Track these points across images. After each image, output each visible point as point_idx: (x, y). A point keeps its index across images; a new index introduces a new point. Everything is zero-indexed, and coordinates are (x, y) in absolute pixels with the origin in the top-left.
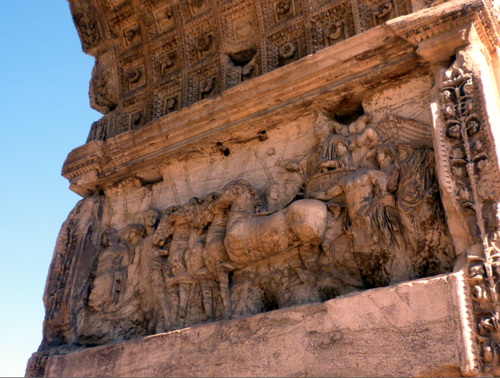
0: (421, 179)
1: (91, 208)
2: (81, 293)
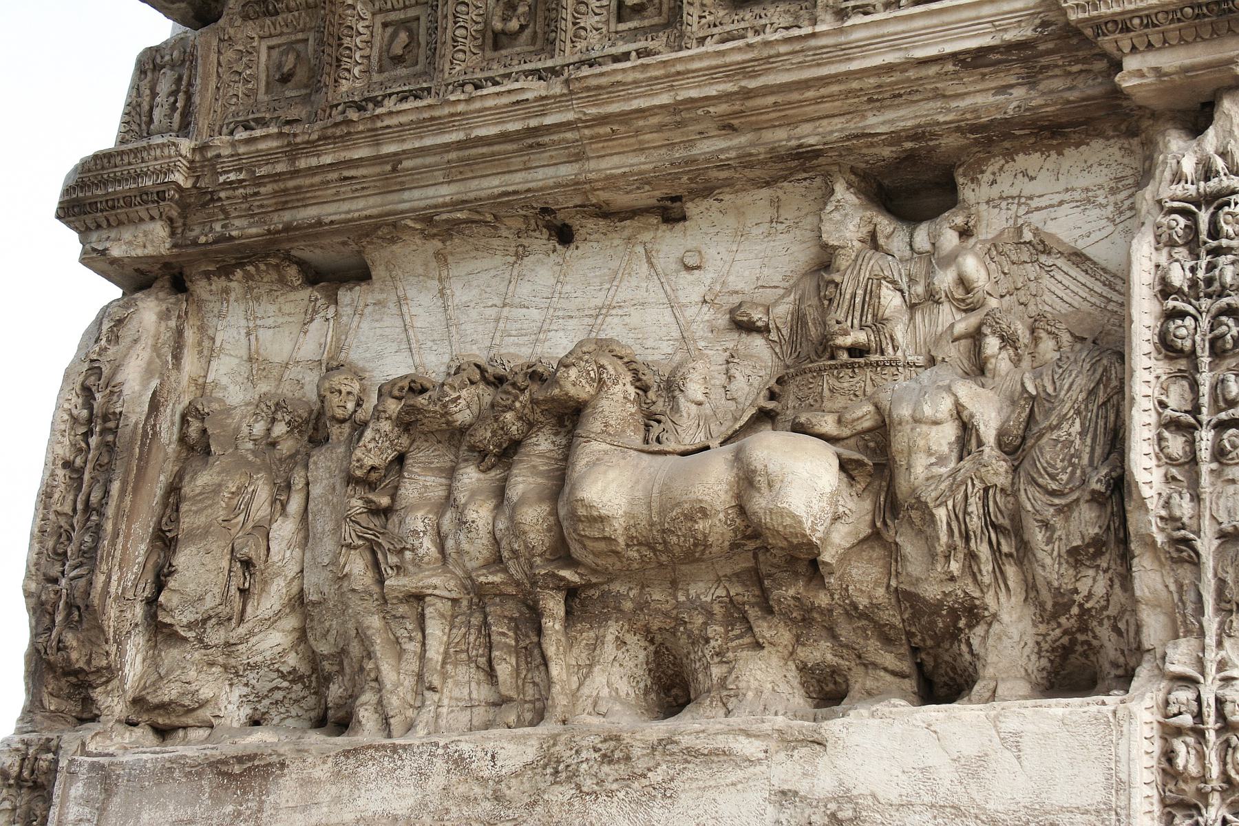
0: (1082, 434)
1: (152, 330)
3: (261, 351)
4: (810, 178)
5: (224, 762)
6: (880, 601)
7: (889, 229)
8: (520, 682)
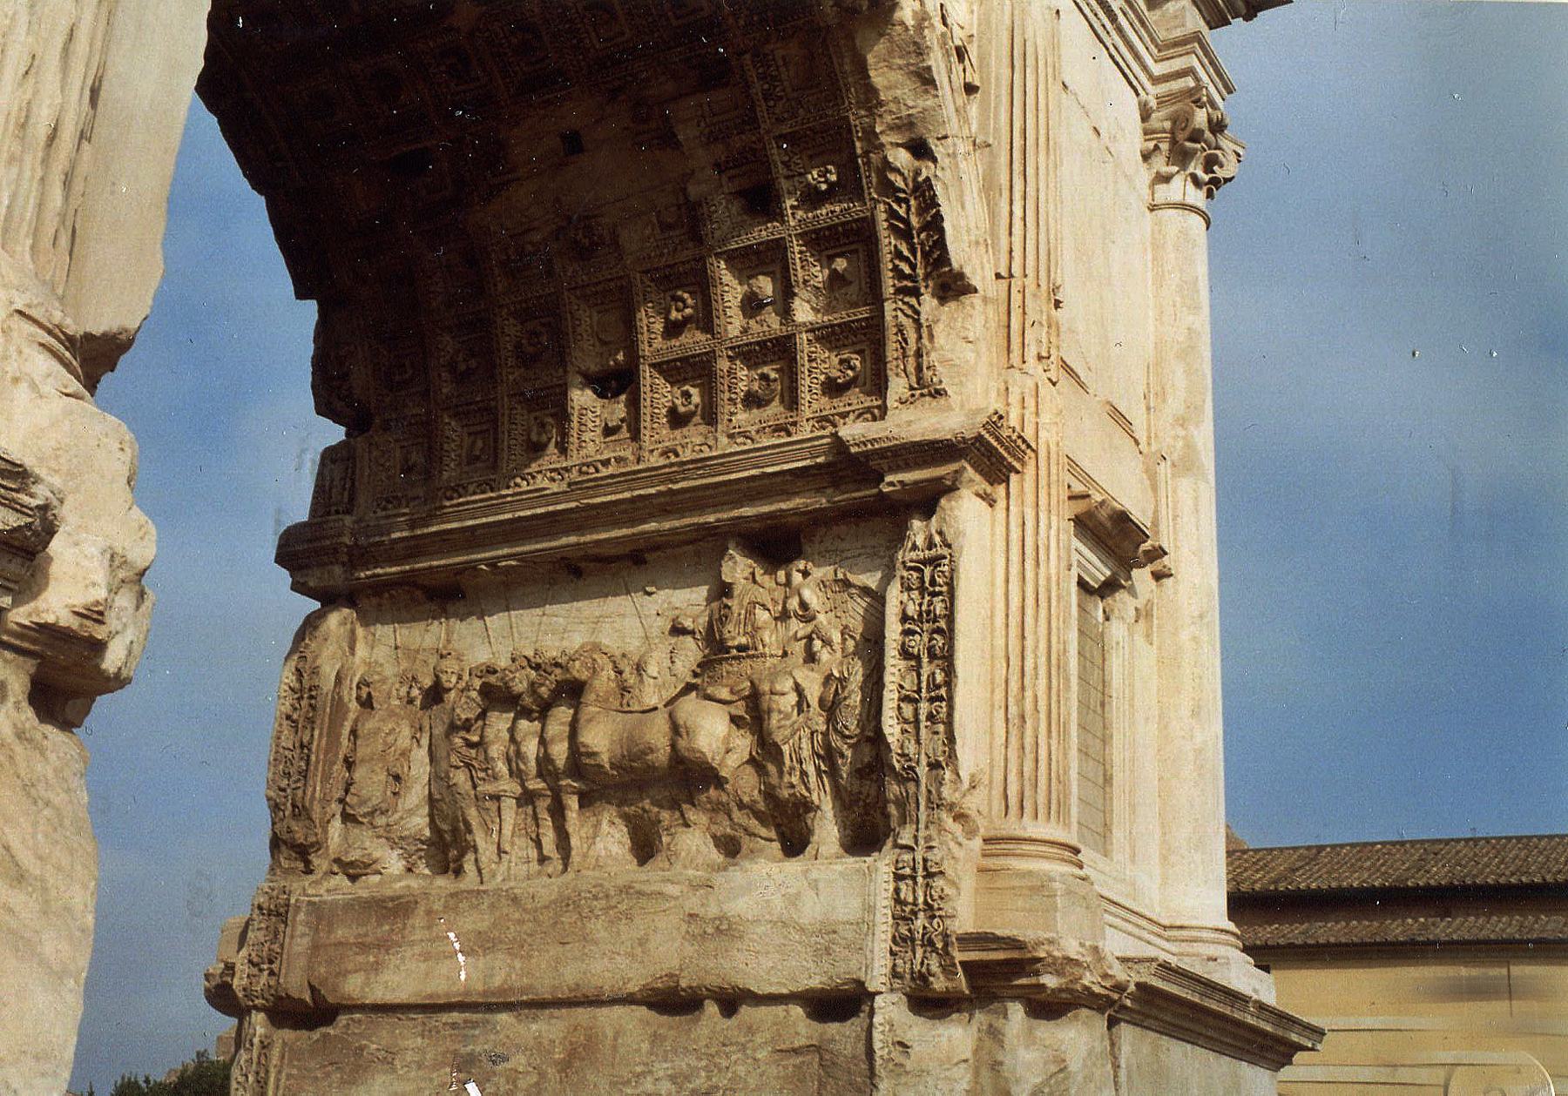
5: (384, 901)
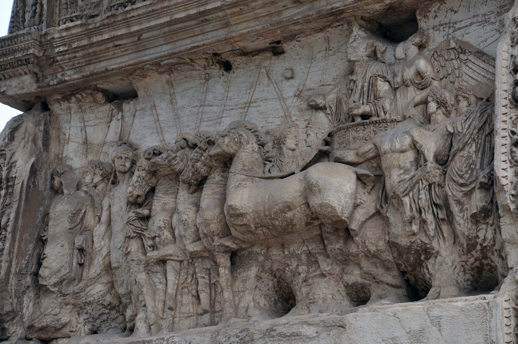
0: (477, 152)
2: (27, 266)
3: (88, 139)
4: (342, 25)
6: (382, 248)
7: (383, 49)
8: (212, 302)
